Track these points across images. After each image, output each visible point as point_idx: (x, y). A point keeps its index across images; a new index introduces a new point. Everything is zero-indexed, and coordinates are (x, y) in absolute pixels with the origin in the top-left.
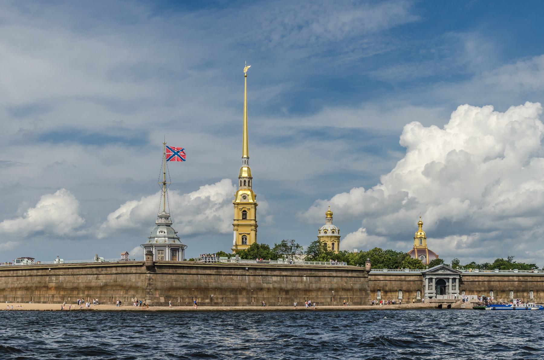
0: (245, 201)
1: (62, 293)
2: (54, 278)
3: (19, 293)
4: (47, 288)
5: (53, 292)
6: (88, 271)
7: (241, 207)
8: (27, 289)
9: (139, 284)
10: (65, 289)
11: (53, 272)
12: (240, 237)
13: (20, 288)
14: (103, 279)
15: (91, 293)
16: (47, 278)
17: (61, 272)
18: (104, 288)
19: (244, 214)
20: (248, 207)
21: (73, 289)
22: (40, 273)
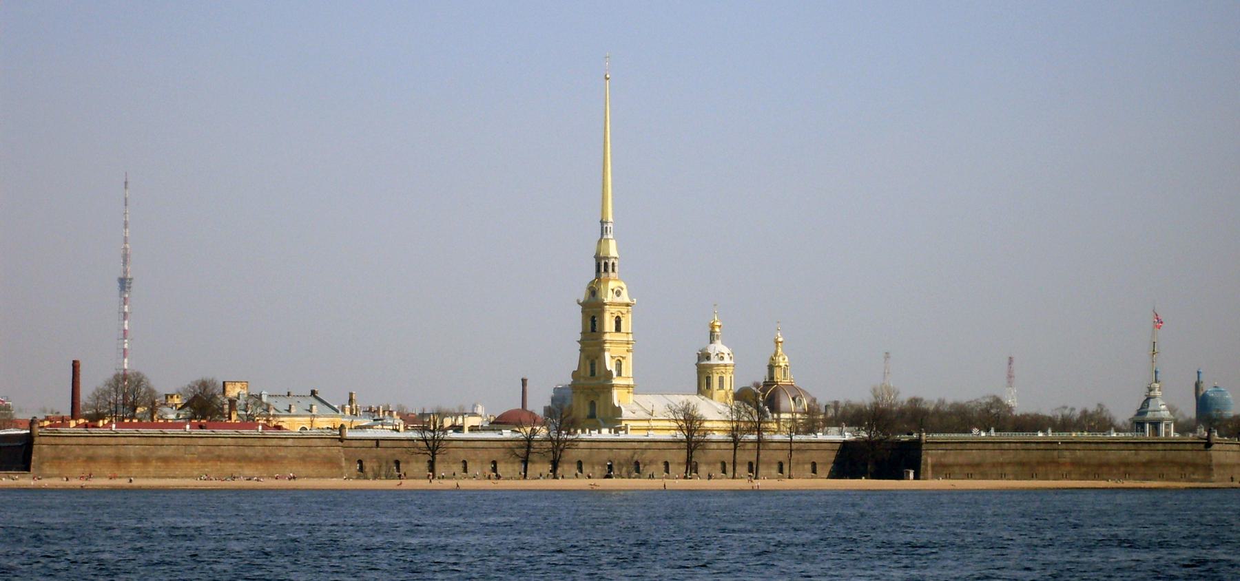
0: (618, 300)
1: (1083, 469)
2: (1067, 453)
3: (1008, 469)
4: (1056, 463)
5: (1068, 468)
6: (1122, 446)
7: (614, 310)
8: (1022, 464)
9: (1199, 461)
10: (1088, 465)
11: (1064, 446)
12: (614, 361)
13: (1009, 463)
14: (1144, 455)
15: (1130, 469)
16: (1056, 453)
17: (1078, 447)
18: (1148, 464)
19: (618, 322)
20: (624, 310)
21: (1101, 465)
22: (1042, 446)
